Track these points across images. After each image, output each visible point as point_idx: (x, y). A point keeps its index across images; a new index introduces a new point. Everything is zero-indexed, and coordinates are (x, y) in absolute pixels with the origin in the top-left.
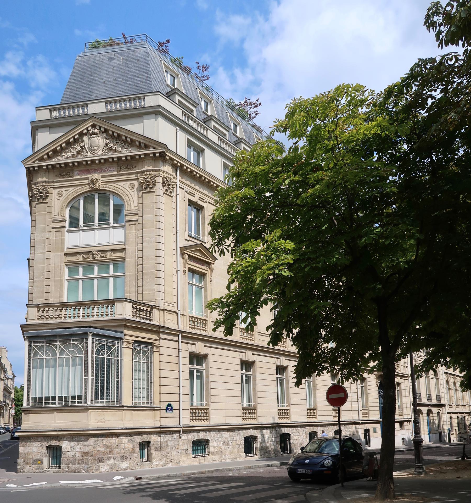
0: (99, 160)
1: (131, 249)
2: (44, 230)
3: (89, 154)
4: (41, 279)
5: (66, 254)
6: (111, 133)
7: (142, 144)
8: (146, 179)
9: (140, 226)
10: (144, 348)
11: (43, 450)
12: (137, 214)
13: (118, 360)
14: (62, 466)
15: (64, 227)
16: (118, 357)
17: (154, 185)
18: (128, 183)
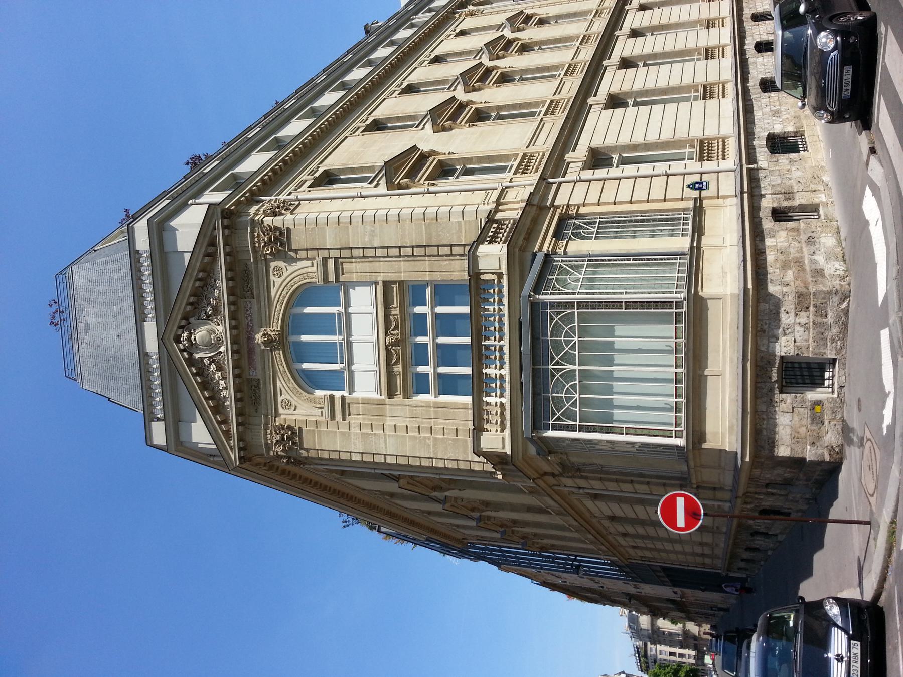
0: (232, 328)
1: (385, 271)
2: (346, 436)
3: (222, 349)
4: (431, 442)
5: (391, 395)
6: (189, 308)
7: (209, 251)
8: (265, 243)
9: (345, 253)
10: (568, 224)
11: (789, 401)
12: (325, 260)
13: (589, 260)
14: (830, 354)
15: (343, 398)
16: (583, 261)
17: (276, 228)
18: (272, 278)
